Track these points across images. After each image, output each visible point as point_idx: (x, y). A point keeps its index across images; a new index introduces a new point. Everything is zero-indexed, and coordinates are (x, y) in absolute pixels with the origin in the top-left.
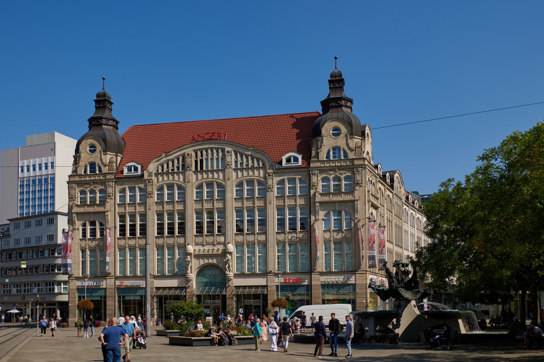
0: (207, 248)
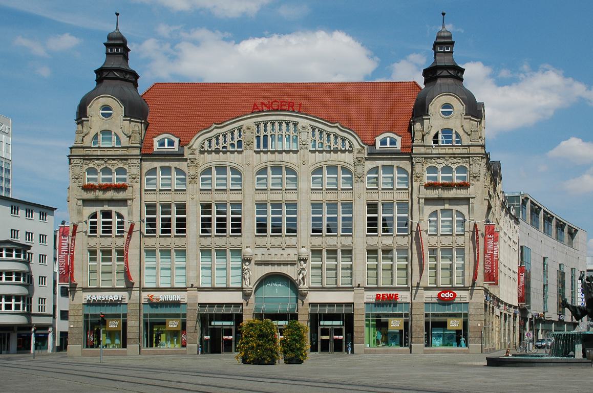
0: (272, 251)
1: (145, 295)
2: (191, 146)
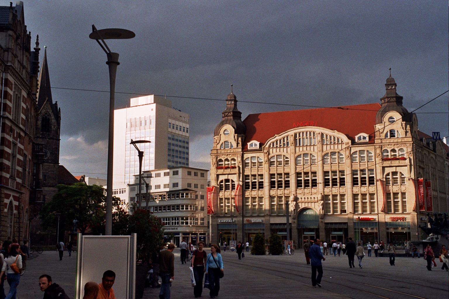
1: (245, 219)
2: (265, 146)
